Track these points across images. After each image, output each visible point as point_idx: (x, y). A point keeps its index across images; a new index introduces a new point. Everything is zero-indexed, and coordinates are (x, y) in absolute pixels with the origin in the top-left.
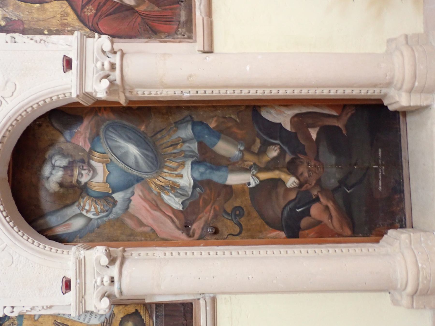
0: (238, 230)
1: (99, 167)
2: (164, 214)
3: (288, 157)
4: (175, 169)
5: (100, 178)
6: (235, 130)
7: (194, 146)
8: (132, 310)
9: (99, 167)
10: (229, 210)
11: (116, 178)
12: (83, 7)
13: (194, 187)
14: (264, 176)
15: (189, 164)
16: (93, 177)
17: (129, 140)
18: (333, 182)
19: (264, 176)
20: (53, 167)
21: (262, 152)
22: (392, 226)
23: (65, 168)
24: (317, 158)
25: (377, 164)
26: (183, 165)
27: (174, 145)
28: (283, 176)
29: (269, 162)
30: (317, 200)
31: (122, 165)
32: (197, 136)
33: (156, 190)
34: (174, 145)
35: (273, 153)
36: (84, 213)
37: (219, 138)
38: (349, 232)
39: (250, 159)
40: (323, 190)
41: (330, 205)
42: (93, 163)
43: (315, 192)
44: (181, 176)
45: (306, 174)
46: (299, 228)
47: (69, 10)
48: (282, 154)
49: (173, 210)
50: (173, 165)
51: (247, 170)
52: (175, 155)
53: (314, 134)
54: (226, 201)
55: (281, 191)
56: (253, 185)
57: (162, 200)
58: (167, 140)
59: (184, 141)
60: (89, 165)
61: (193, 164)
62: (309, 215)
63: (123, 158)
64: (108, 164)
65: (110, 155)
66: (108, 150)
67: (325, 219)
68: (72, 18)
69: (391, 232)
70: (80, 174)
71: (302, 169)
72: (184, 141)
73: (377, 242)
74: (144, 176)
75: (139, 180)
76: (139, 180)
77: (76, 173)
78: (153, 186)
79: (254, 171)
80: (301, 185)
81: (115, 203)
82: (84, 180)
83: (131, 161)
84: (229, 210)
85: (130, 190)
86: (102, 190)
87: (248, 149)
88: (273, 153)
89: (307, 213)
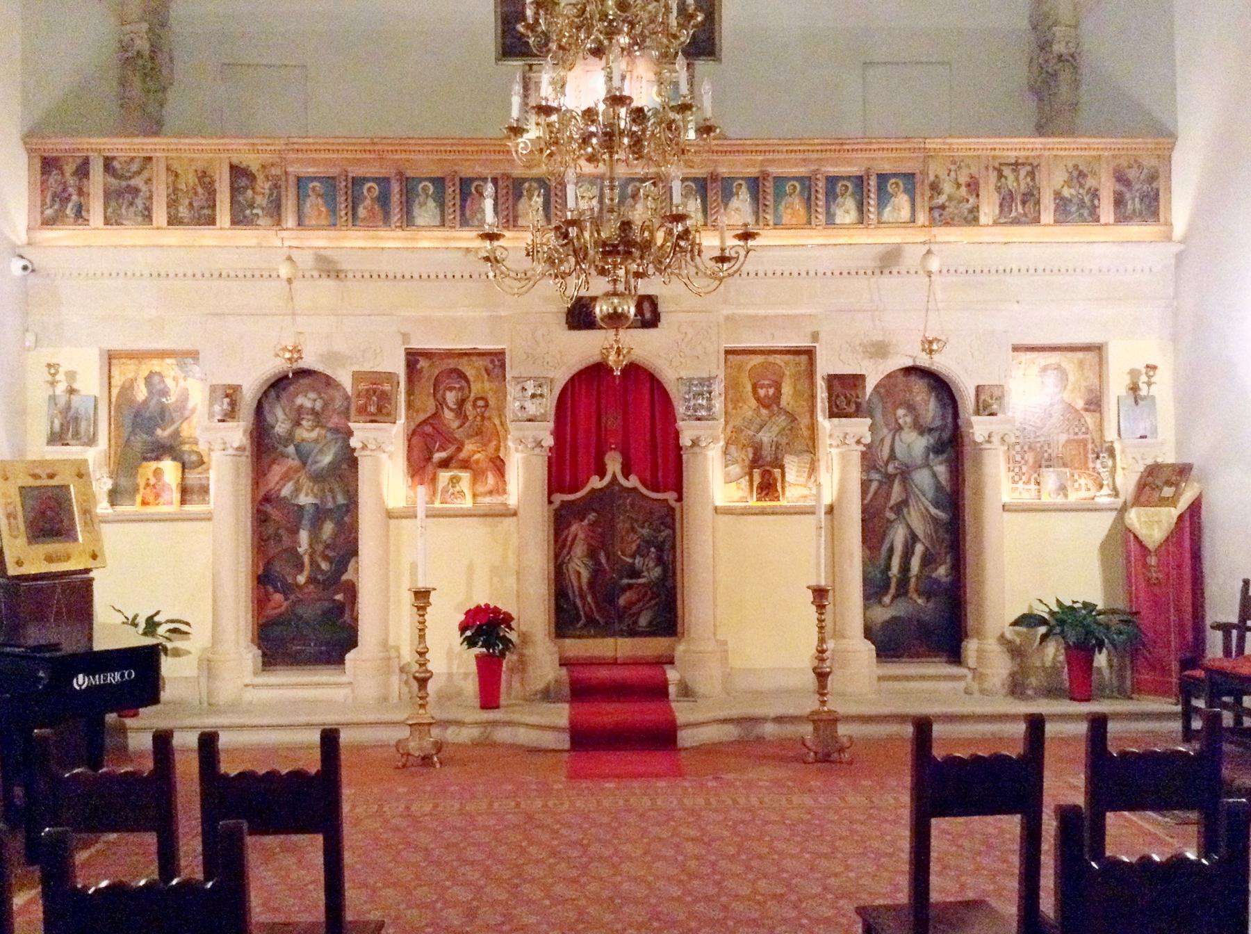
0: (265, 537)
1: (314, 434)
2: (278, 483)
3: (320, 577)
4: (312, 490)
5: (306, 435)
6: (343, 537)
7: (330, 505)
8: (205, 459)
9: (314, 434)
10: (280, 531)
11: (306, 447)
12: (431, 424)
13: (298, 505)
14: (306, 560)
15: (315, 501)
16: (307, 430)
17: (336, 455)
18: (300, 610)
19: (306, 560)
20: (315, 400)
21: (326, 558)
22: (264, 655)
23: (313, 409)
24: (320, 599)
25: (315, 645)
26: (315, 496)
27: (331, 490)
28: (306, 573)
29: (316, 562)
30: (286, 600)
31: (315, 451)
32: (339, 507)
33: (296, 477)
34: (331, 490)
35: (324, 566)
36: (279, 424)
37: (336, 524)
38: (260, 622)
39: (320, 547)
40: (294, 603)
41: (283, 608)
42: (318, 429)
43: (292, 597)
44: (307, 495)
45: (306, 590)
46: (264, 585)
47: (429, 414)
48: (322, 571)
49: (280, 490)
50: (315, 491)
51: (311, 545)
52: (323, 491)
53: (339, 597)
54: (287, 529)
55: (294, 571)
56: (299, 550)
57: (289, 481)
58: (336, 486)
59: (334, 498)
60: (316, 427)
61: (315, 504)
62: (276, 592)
63: (321, 451)
64: (316, 441)
65: (324, 442)
66: (328, 439)
67: (272, 604)
68: (422, 417)
69: (260, 652)
70: (309, 420)
71: (311, 587)
72: (334, 498)
73: (253, 641)
74: (308, 467)
75: (304, 464)
76: (304, 464)
77: (309, 417)
78: (299, 474)
79: (310, 551)
80: (298, 586)
81: (286, 447)
82: (304, 423)
83: (319, 458)
84: (280, 531)
85: (296, 458)
86: (296, 437)
87: (327, 547)
88: (324, 566)
89: (277, 591)
